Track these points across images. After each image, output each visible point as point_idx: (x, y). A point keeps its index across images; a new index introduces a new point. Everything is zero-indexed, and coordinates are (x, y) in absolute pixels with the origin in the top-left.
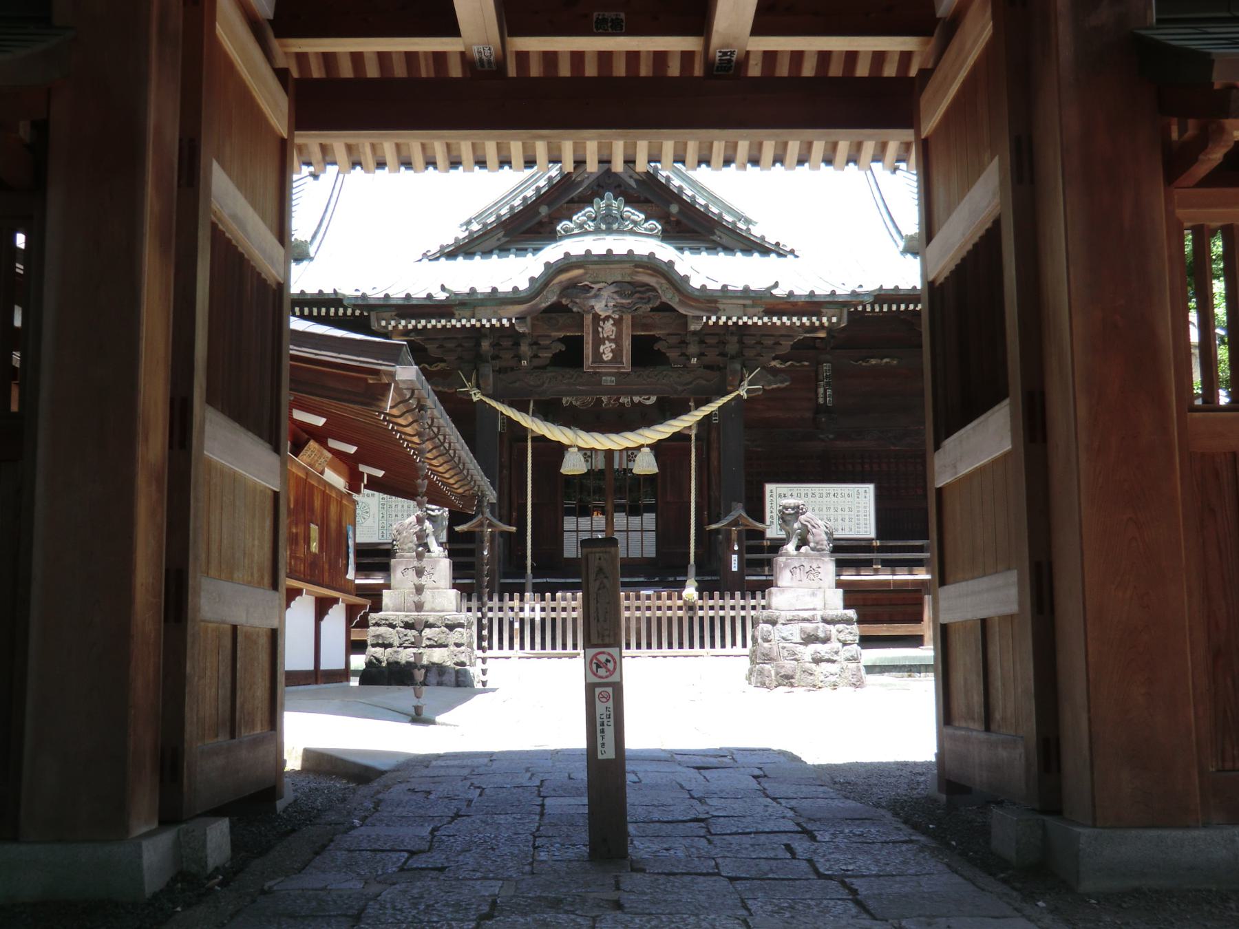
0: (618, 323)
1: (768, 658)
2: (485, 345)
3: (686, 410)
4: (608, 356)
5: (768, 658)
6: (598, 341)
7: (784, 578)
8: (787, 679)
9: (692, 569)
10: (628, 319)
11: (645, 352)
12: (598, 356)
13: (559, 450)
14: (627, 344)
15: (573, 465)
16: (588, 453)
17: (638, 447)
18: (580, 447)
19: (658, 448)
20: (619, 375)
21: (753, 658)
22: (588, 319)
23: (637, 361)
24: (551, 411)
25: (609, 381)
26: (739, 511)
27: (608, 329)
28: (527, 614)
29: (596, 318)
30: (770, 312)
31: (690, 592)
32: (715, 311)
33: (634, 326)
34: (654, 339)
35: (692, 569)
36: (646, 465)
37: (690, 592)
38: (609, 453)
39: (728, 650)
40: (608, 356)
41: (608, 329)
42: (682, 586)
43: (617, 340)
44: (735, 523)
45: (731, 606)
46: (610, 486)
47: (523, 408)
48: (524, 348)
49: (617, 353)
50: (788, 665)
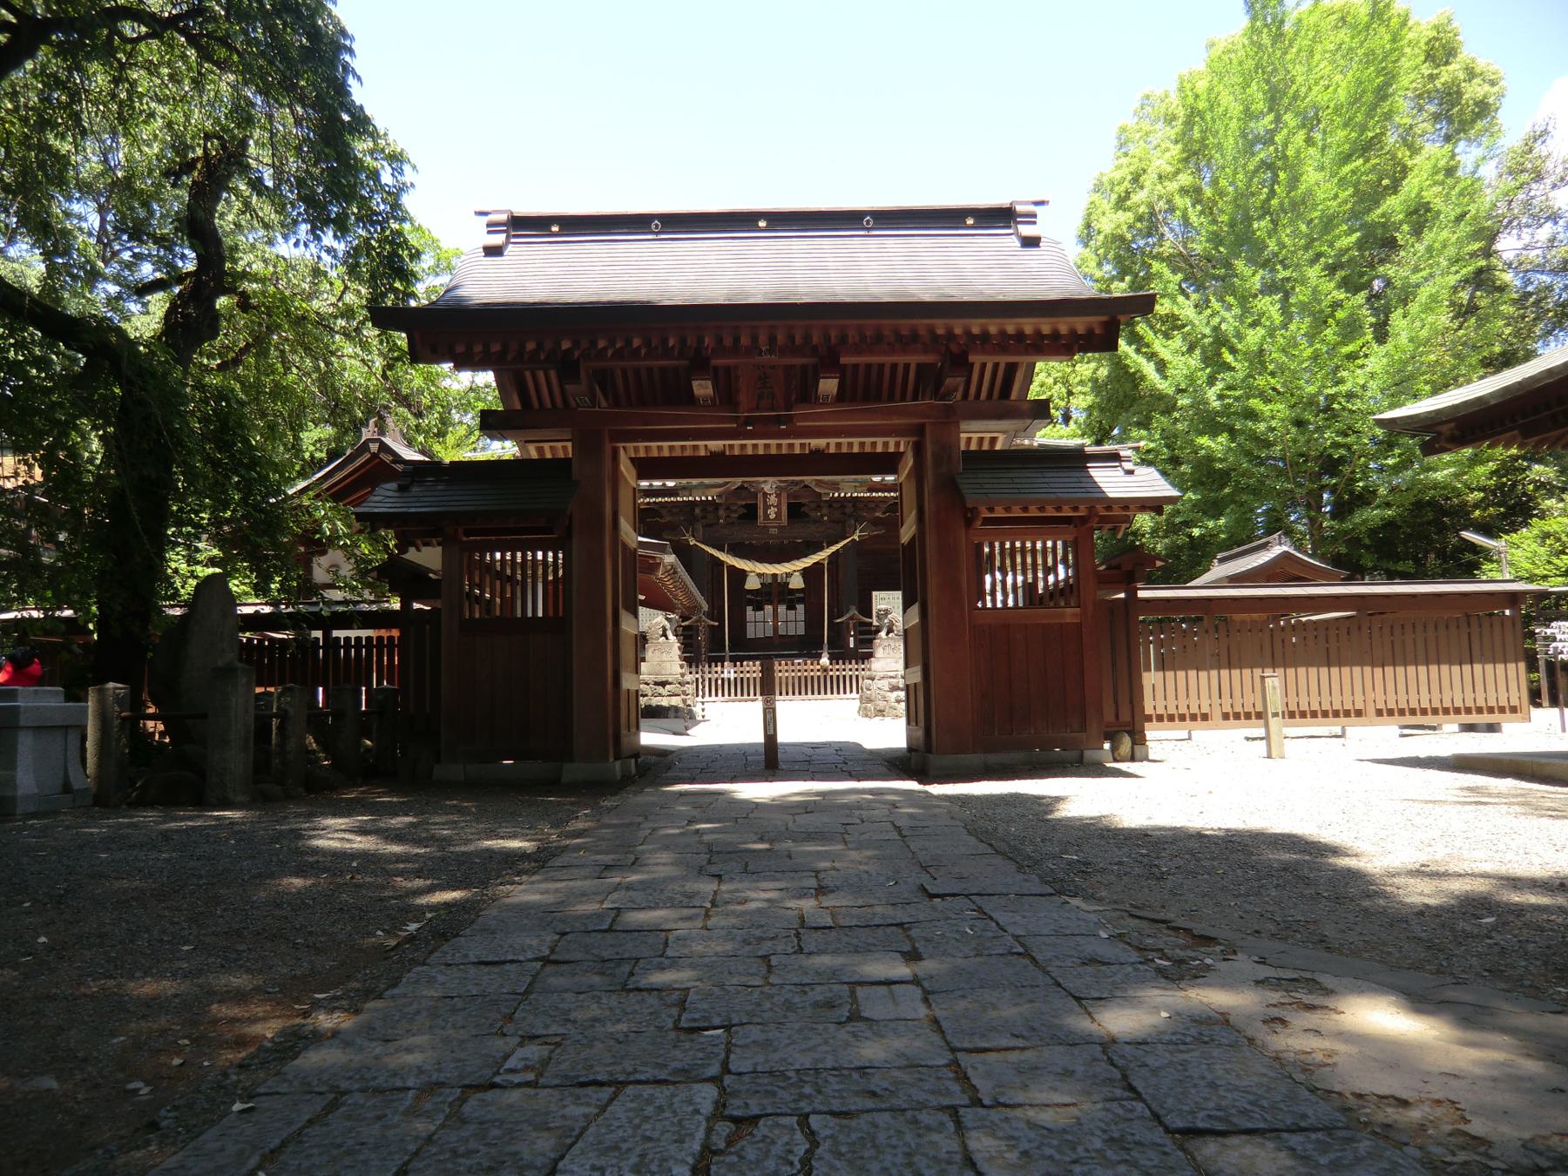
0: (778, 496)
1: (870, 700)
2: (697, 511)
3: (822, 549)
4: (773, 516)
5: (870, 700)
6: (767, 507)
7: (879, 653)
8: (881, 713)
9: (826, 646)
10: (784, 495)
11: (795, 511)
12: (766, 516)
13: (743, 574)
14: (784, 508)
15: (752, 583)
16: (760, 575)
17: (792, 571)
18: (756, 572)
19: (805, 572)
20: (780, 528)
21: (861, 699)
22: (760, 495)
23: (790, 516)
24: (737, 551)
25: (774, 531)
26: (854, 611)
27: (773, 500)
28: (726, 675)
29: (765, 495)
30: (871, 490)
31: (825, 661)
32: (838, 490)
33: (789, 496)
34: (802, 505)
35: (826, 646)
36: (797, 583)
37: (825, 661)
38: (775, 576)
39: (848, 695)
40: (773, 516)
41: (773, 500)
42: (819, 656)
43: (778, 506)
44: (852, 618)
45: (849, 669)
47: (721, 549)
48: (721, 512)
49: (778, 514)
50: (881, 704)
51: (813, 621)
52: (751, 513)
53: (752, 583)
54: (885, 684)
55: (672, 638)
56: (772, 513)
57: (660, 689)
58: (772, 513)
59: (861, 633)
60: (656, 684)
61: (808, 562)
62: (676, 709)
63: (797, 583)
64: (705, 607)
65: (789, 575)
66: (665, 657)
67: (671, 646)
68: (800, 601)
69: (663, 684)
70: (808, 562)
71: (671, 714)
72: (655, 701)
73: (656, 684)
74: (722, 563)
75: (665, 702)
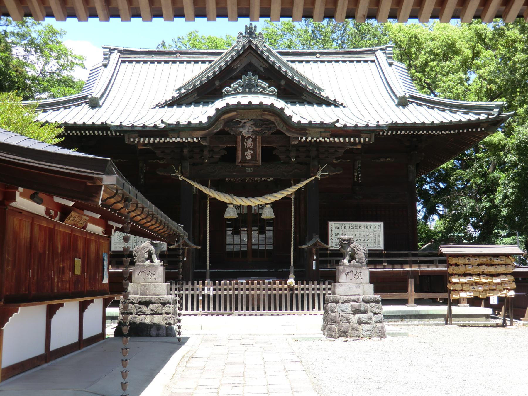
0: (254, 140)
1: (334, 322)
2: (186, 151)
3: (289, 186)
4: (249, 157)
5: (334, 322)
6: (244, 150)
7: (342, 278)
8: (344, 333)
9: (292, 269)
10: (259, 139)
11: (268, 155)
12: (244, 157)
13: (224, 206)
14: (259, 151)
15: (231, 214)
16: (237, 207)
17: (264, 203)
18: (235, 203)
19: (275, 205)
20: (254, 167)
22: (239, 138)
23: (263, 160)
24: (219, 186)
25: (249, 170)
26: (316, 239)
27: (249, 143)
28: (206, 292)
29: (243, 138)
31: (291, 281)
33: (263, 141)
34: (273, 149)
35: (292, 269)
36: (268, 214)
37: (291, 281)
38: (249, 207)
39: (311, 311)
40: (249, 157)
41: (249, 143)
42: (287, 278)
43: (254, 149)
44: (315, 245)
45: (313, 288)
46: (249, 219)
47: (205, 184)
48: (206, 153)
49: (254, 156)
51: (281, 240)
52: (230, 156)
53: (231, 214)
54: (347, 307)
55: (156, 261)
56: (248, 154)
57: (144, 308)
58: (248, 154)
59: (322, 255)
60: (140, 303)
61: (278, 196)
62: (158, 326)
63: (268, 214)
64: (185, 235)
65: (262, 207)
66: (149, 279)
67: (156, 268)
68: (269, 225)
69: (147, 303)
70: (278, 196)
71: (153, 332)
72: (139, 319)
73: (140, 303)
74: (206, 196)
75: (148, 320)
